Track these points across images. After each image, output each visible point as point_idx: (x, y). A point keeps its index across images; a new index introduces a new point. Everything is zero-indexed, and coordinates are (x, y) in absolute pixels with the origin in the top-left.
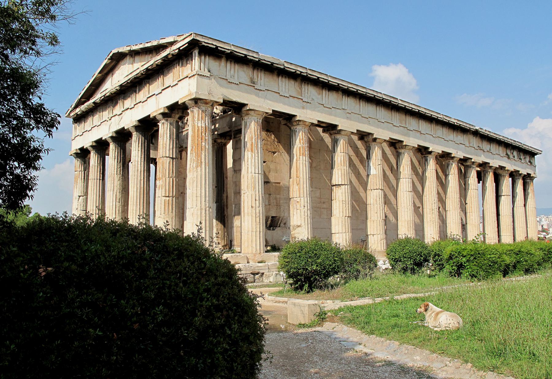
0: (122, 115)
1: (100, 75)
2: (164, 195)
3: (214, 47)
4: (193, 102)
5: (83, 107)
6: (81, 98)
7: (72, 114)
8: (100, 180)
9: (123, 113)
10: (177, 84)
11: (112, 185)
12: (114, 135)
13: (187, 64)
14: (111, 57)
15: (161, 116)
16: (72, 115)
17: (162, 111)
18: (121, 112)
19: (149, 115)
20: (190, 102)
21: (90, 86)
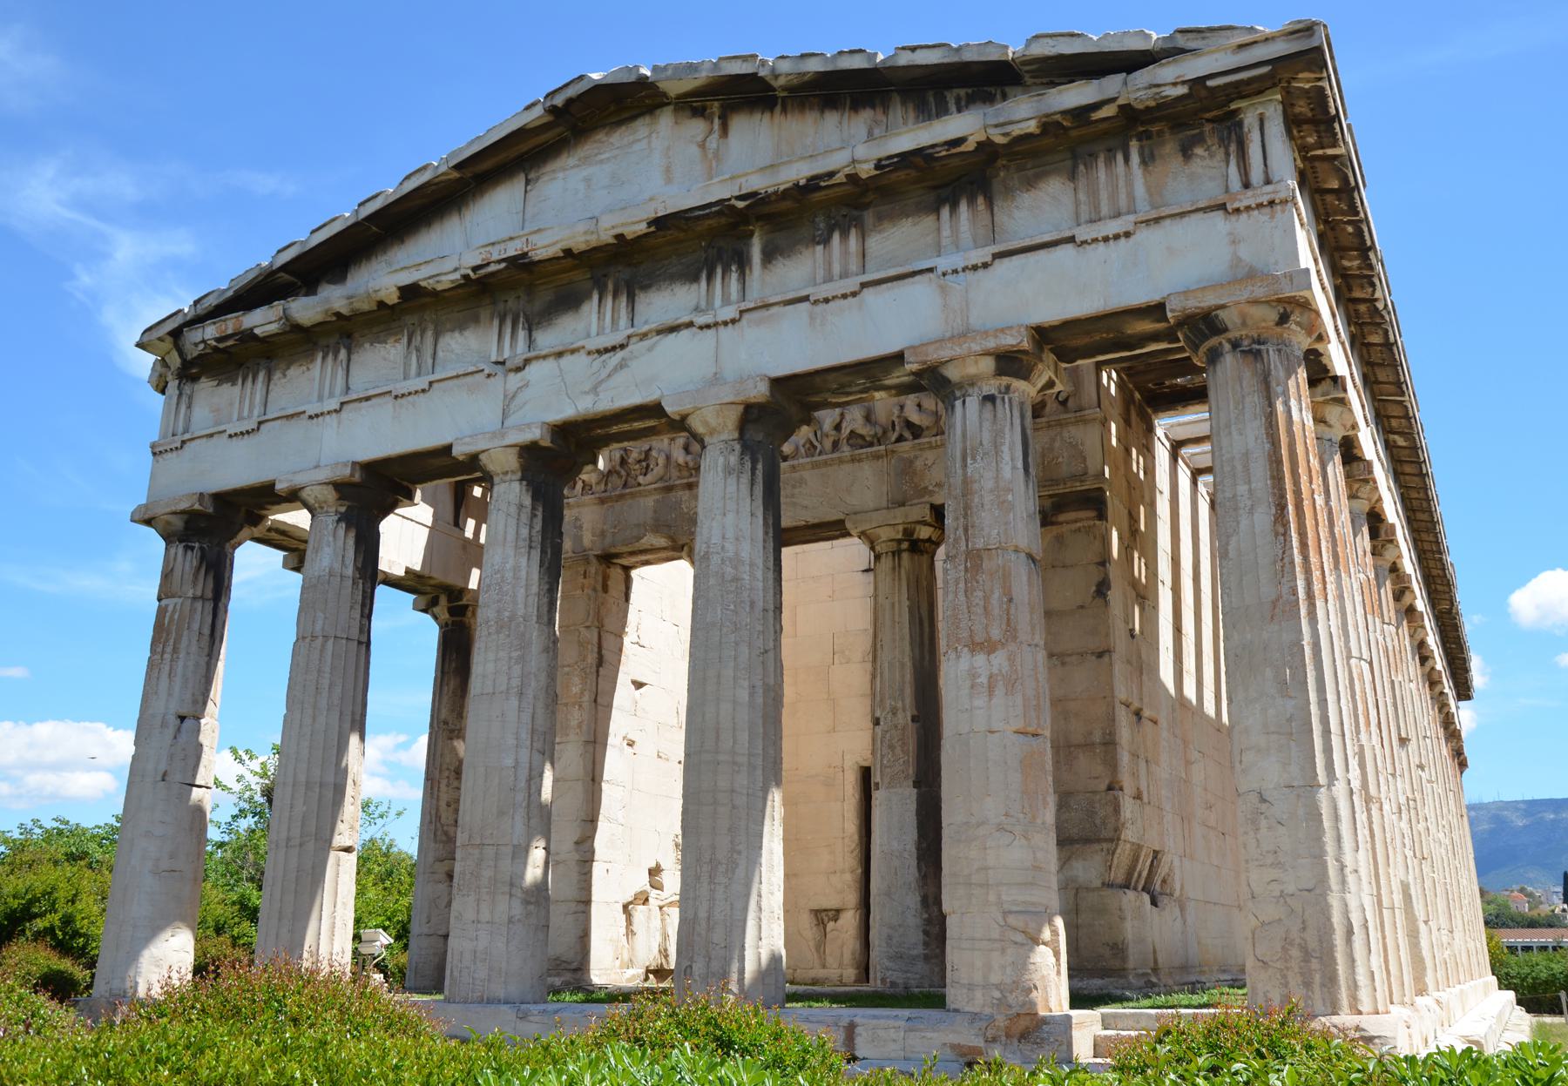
0: (620, 354)
1: (456, 175)
2: (1019, 725)
3: (1333, 112)
4: (1273, 316)
5: (305, 309)
6: (284, 268)
7: (210, 331)
8: (360, 643)
9: (635, 347)
10: (1127, 235)
11: (517, 670)
12: (546, 443)
13: (1186, 153)
14: (570, 102)
15: (988, 365)
16: (194, 336)
17: (1009, 341)
18: (618, 338)
19: (899, 358)
20: (1257, 312)
21: (369, 218)
